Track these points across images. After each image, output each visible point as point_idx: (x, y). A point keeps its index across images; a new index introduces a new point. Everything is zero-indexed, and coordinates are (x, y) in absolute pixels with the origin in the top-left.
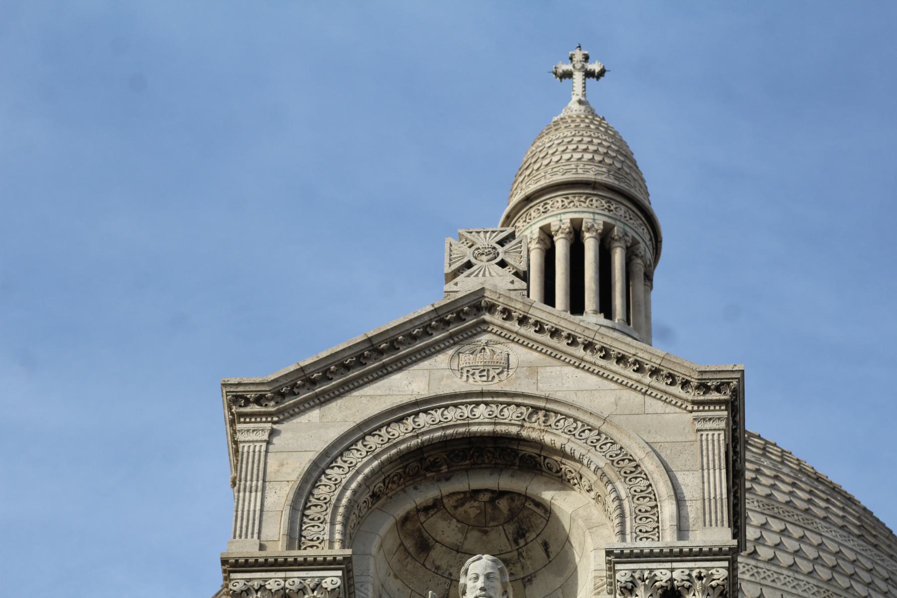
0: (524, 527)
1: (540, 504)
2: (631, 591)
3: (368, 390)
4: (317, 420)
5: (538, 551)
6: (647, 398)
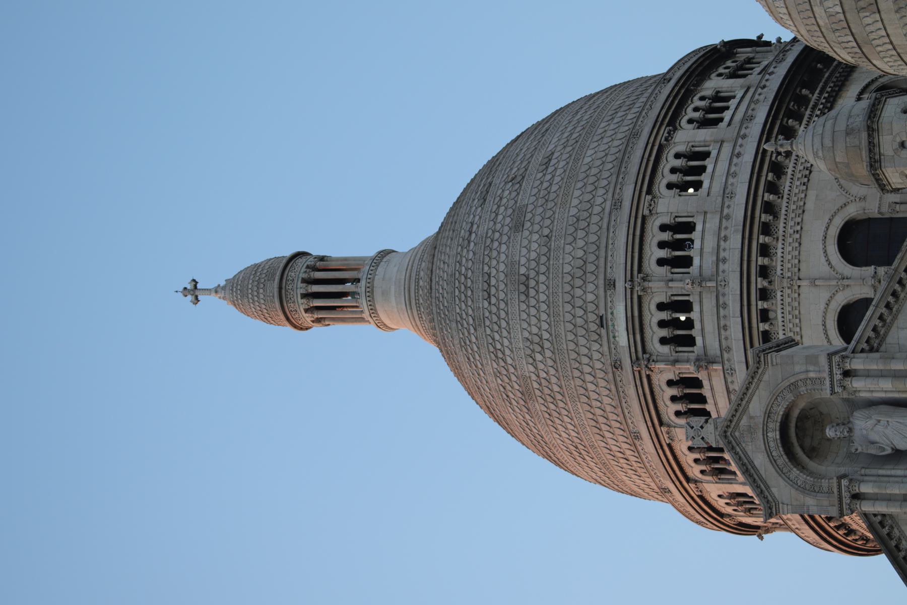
1: (800, 413)
2: (844, 387)
3: (762, 472)
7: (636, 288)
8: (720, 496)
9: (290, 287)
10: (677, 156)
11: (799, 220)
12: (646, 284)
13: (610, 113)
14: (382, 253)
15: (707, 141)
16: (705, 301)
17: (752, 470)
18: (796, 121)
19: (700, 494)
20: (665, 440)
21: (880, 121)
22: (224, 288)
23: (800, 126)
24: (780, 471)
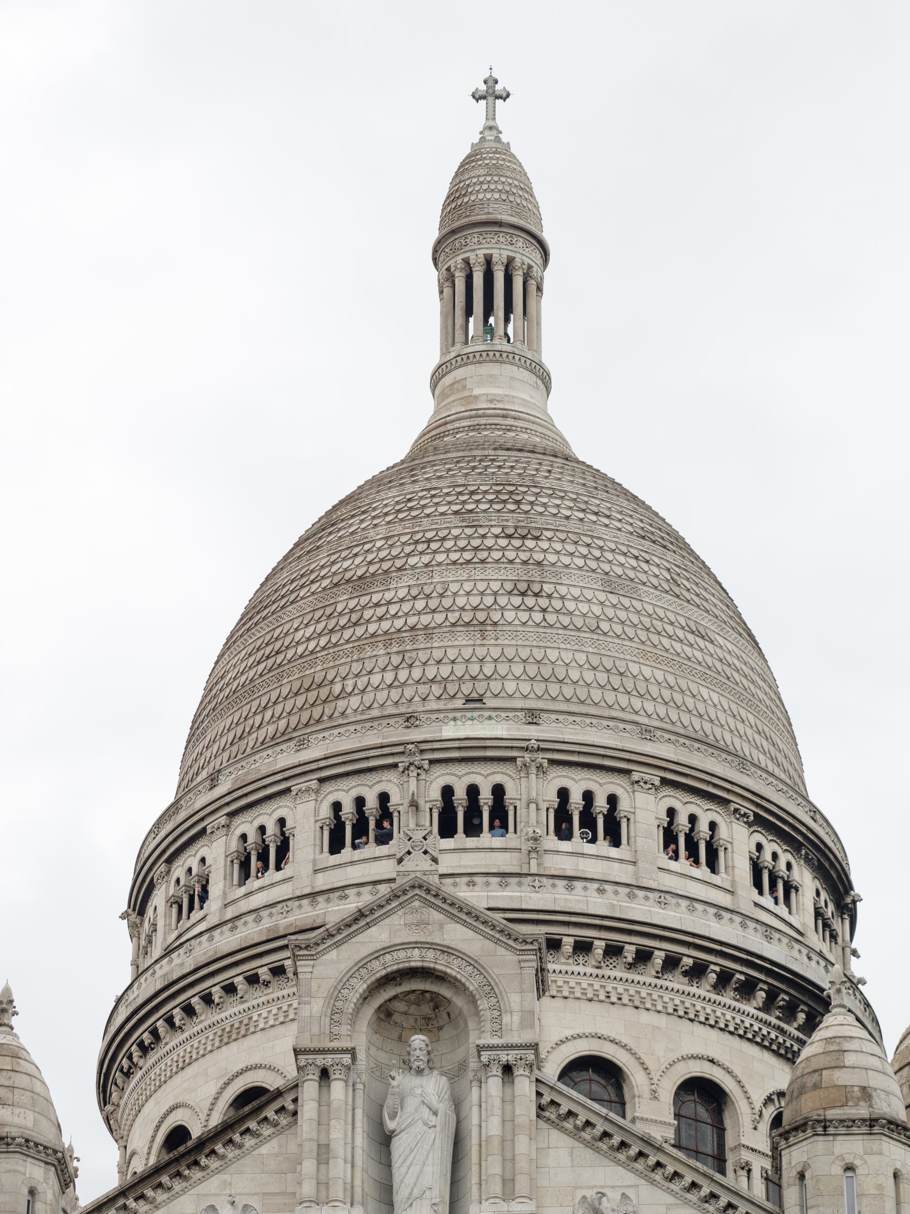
2: (488, 1066)
3: (360, 938)
4: (335, 958)
5: (445, 1016)
7: (527, 756)
8: (203, 860)
9: (501, 239)
10: (713, 826)
11: (625, 1000)
12: (533, 770)
13: (766, 729)
14: (547, 378)
15: (733, 869)
16: (507, 855)
18: (764, 1003)
19: (209, 831)
20: (297, 785)
21: (884, 1138)
22: (498, 140)
23: (755, 1008)
24: (363, 964)
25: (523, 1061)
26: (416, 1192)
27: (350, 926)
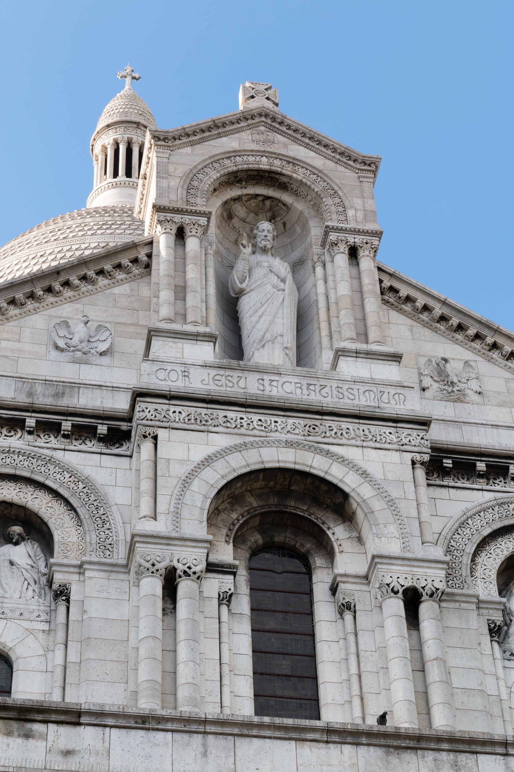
0: (275, 214)
1: (284, 205)
2: (336, 245)
3: (212, 142)
4: (190, 153)
6: (337, 165)
17: (216, 132)
25: (369, 245)
26: (268, 336)
27: (203, 131)
